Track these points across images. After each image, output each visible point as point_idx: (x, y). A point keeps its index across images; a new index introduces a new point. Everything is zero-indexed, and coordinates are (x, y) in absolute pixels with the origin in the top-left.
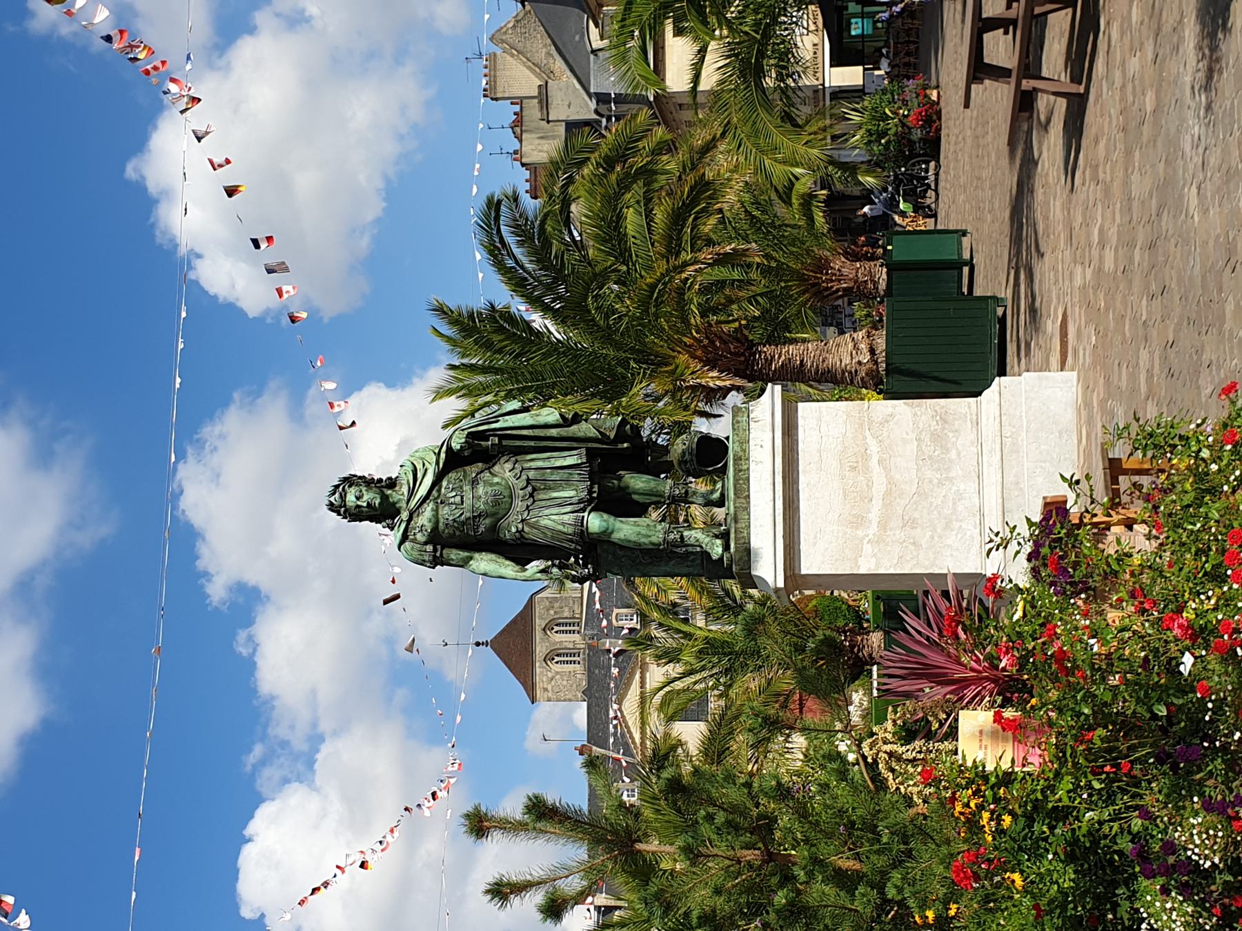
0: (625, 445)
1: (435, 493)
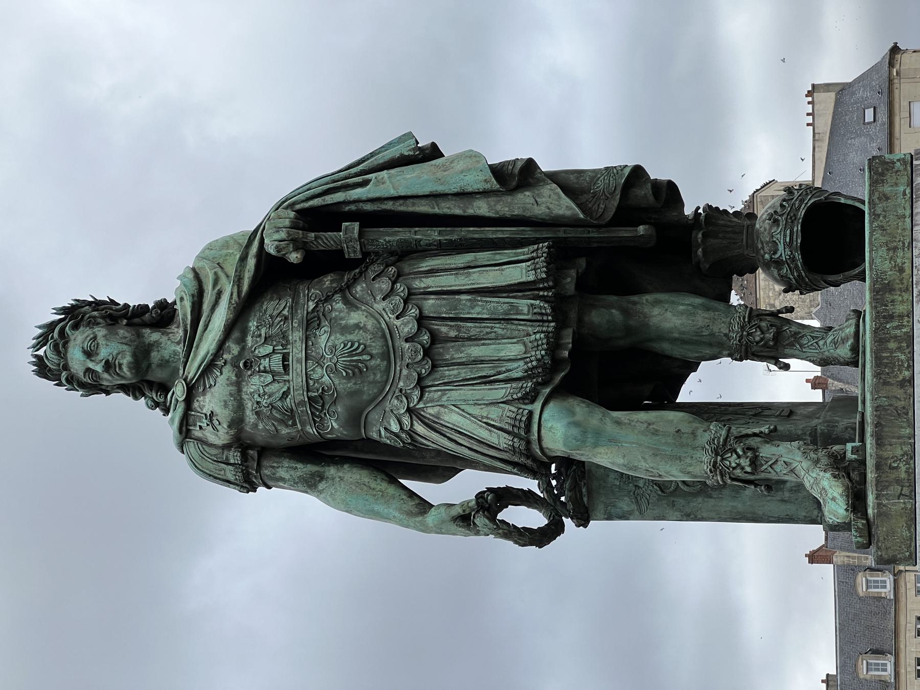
0: (641, 229)
1: (234, 348)
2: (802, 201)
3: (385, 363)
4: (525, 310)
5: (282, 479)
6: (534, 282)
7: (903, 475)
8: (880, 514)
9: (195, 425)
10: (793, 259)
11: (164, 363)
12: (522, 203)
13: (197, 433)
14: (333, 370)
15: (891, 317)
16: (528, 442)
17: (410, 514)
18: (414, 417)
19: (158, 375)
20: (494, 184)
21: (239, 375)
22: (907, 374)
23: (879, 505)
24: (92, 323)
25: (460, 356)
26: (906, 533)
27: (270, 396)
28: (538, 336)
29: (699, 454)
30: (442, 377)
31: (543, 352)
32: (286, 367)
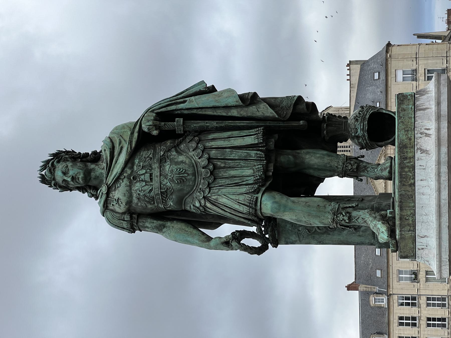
2: (367, 112)
3: (194, 177)
4: (254, 155)
5: (147, 227)
6: (257, 144)
7: (411, 222)
8: (401, 238)
9: (110, 204)
10: (364, 136)
11: (97, 178)
12: (252, 111)
13: (111, 207)
14: (172, 180)
15: (406, 158)
16: (256, 210)
17: (203, 241)
18: (206, 200)
19: (94, 183)
20: (240, 103)
21: (131, 182)
22: (412, 181)
23: (401, 234)
24: (66, 160)
25: (226, 175)
26: (412, 246)
27: (144, 191)
28: (259, 166)
29: (327, 215)
30: (219, 183)
31: (261, 173)
32: (151, 179)
